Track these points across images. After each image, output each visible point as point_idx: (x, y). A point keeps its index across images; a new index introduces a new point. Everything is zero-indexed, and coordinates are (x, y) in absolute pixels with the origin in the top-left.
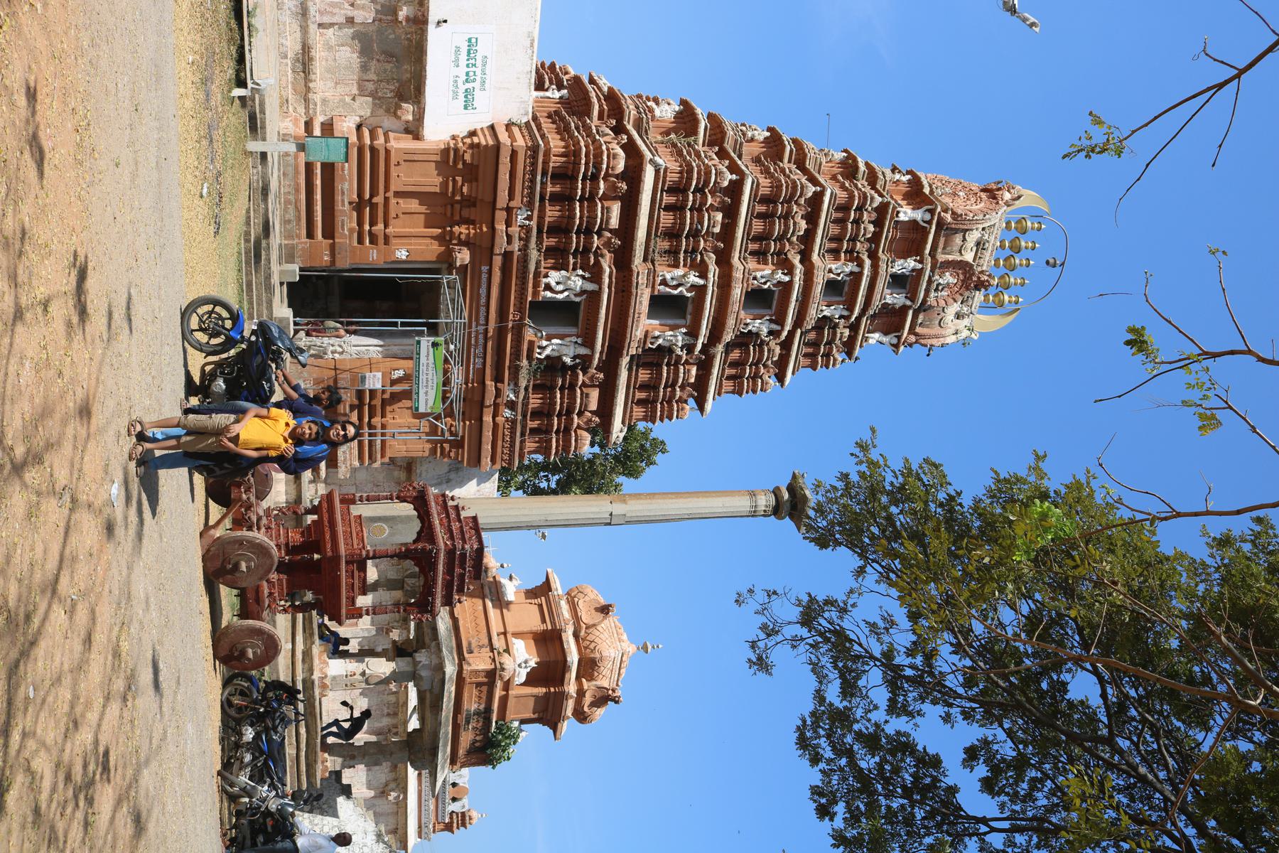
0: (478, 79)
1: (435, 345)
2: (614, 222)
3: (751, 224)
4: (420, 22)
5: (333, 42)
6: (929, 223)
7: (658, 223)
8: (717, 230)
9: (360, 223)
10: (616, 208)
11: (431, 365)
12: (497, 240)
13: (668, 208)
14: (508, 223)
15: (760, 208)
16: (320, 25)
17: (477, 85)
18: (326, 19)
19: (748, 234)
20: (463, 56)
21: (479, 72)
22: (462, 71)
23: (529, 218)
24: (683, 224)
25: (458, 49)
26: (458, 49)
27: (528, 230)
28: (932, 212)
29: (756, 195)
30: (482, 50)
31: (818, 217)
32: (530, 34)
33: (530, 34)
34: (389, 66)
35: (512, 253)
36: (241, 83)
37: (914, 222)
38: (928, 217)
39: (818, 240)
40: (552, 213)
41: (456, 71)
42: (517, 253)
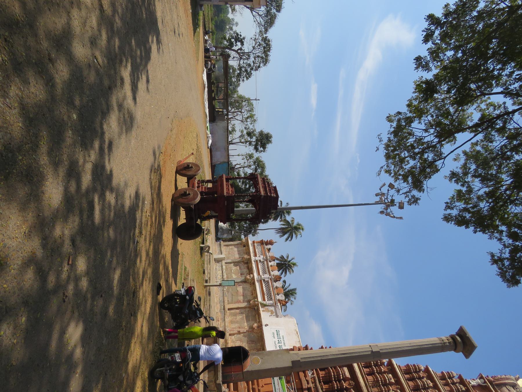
0: (282, 342)
1: (280, 379)
2: (348, 375)
3: (407, 383)
4: (260, 327)
5: (234, 340)
6: (485, 382)
7: (367, 380)
8: (393, 381)
9: (248, 385)
10: (346, 369)
11: (281, 389)
12: (303, 382)
13: (368, 375)
14: (305, 376)
15: (407, 376)
16: (230, 335)
17: (282, 344)
18: (232, 332)
19: (409, 387)
20: (276, 335)
21: (282, 340)
22: (276, 340)
23: (313, 374)
24: (377, 378)
25: (273, 333)
26: (273, 333)
27: (314, 378)
28: (481, 377)
29: (401, 370)
30: (281, 334)
31: (433, 378)
32: (295, 330)
33: (295, 330)
34: (253, 345)
35: (311, 388)
36: (203, 243)
37: (479, 385)
38: (482, 380)
39: (441, 387)
40: (322, 373)
41: (274, 340)
42: (313, 389)
